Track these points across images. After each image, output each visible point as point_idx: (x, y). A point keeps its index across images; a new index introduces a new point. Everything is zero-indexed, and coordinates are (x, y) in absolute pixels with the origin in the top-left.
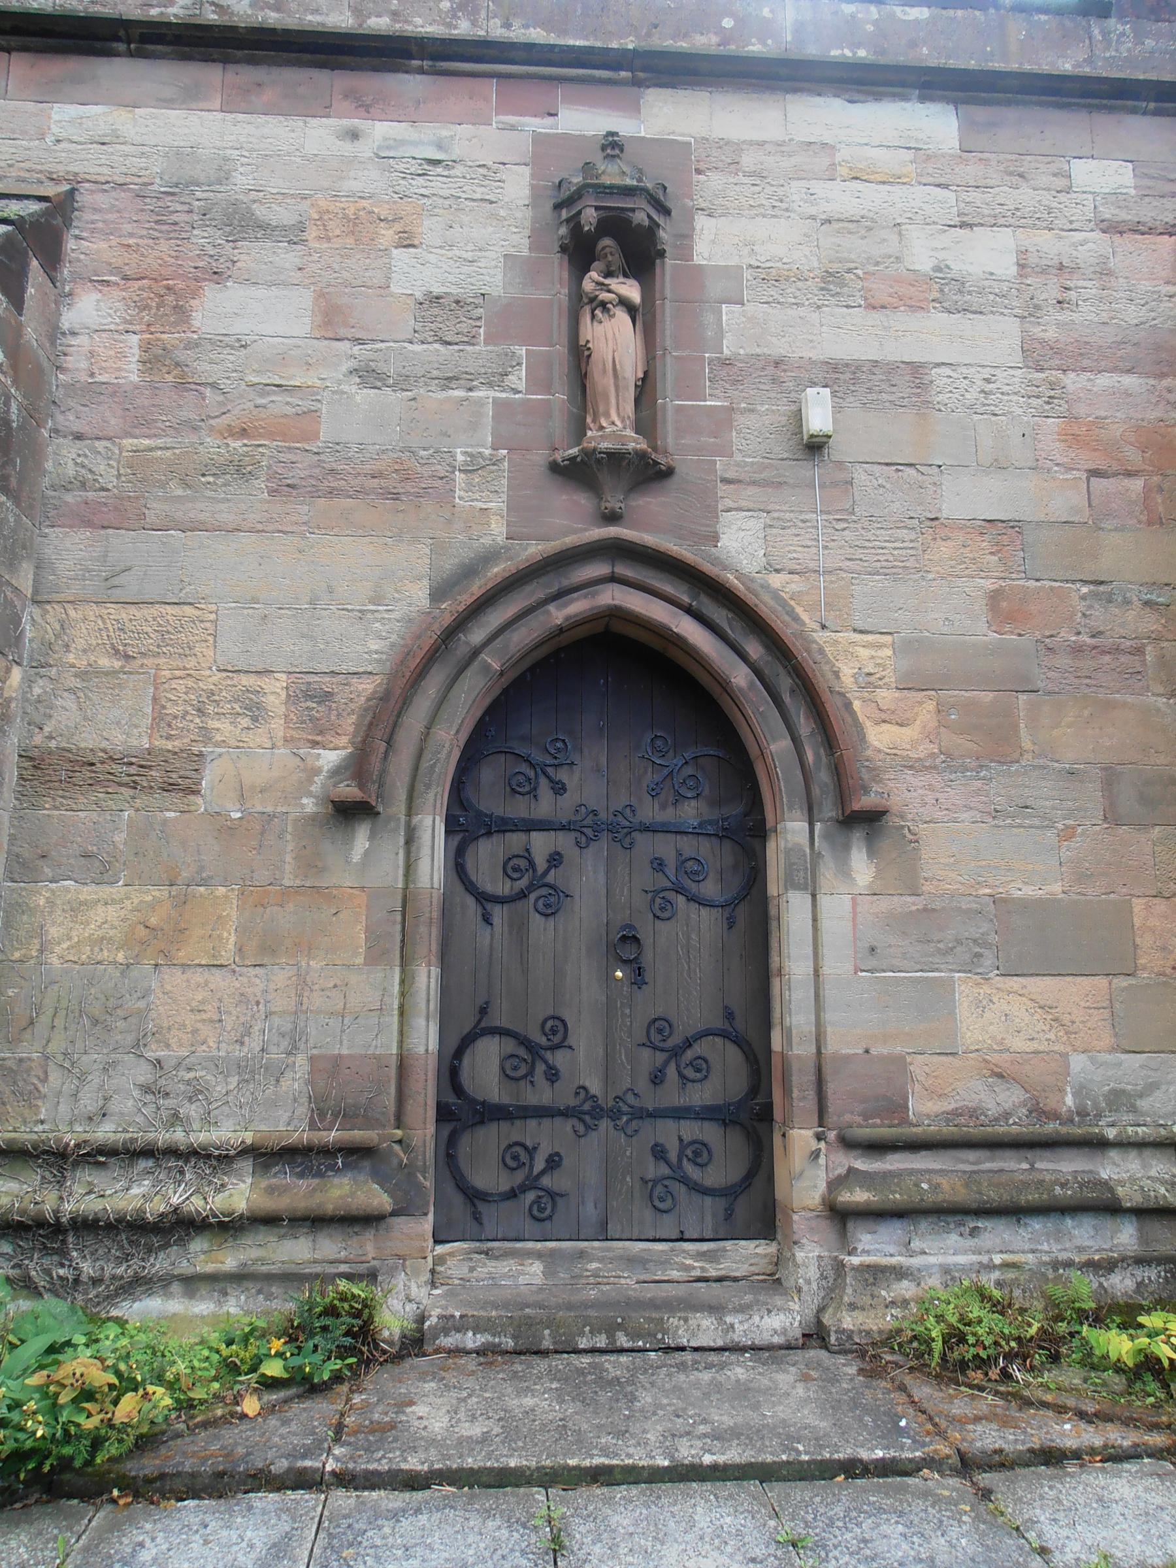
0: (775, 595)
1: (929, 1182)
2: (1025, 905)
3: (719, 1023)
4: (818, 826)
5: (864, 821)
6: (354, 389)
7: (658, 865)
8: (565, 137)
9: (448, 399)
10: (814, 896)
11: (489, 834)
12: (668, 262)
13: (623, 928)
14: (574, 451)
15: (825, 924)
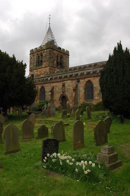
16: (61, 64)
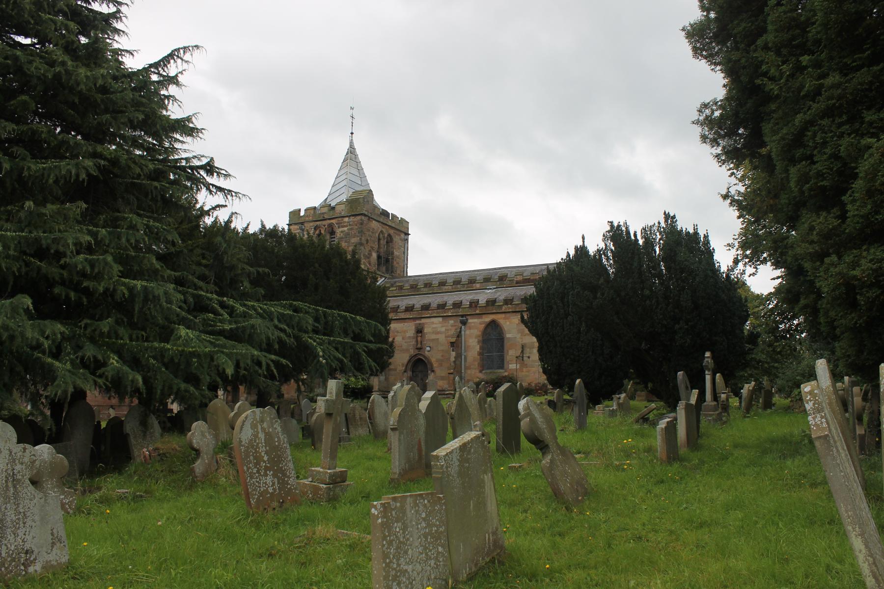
5: (433, 371)
16: (387, 261)
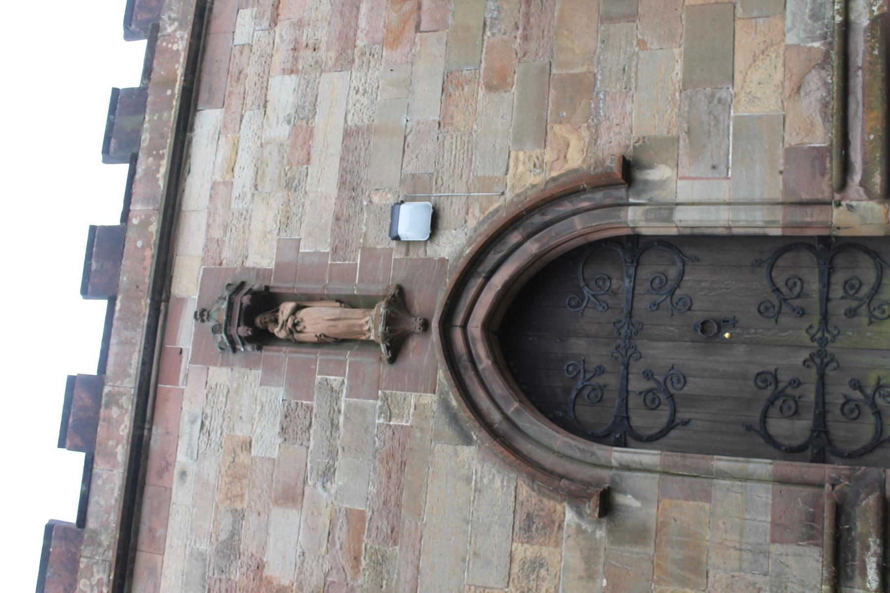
0: (481, 223)
1: (869, 134)
2: (688, 70)
3: (764, 270)
4: (631, 200)
5: (629, 170)
6: (334, 486)
7: (656, 306)
8: (195, 343)
9: (345, 426)
10: (678, 204)
11: (628, 418)
12: (272, 283)
13: (696, 330)
14: (383, 347)
15: (696, 197)
